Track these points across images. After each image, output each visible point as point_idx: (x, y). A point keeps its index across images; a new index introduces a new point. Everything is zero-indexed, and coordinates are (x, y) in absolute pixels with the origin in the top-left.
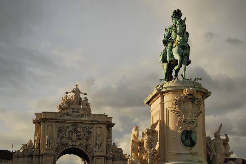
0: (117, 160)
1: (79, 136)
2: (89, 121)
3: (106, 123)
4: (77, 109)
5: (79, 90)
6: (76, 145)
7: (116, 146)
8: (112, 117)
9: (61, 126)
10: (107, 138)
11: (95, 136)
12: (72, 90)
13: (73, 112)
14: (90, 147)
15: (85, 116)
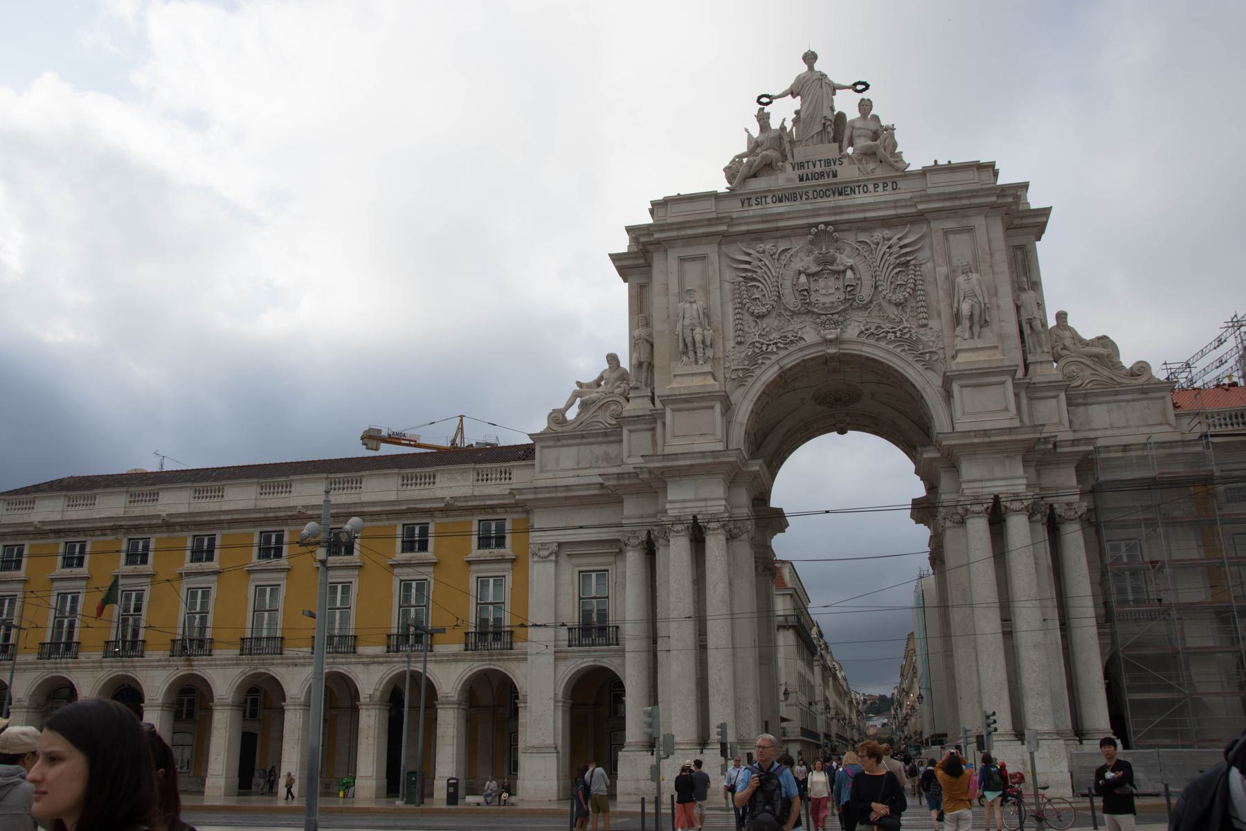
0: (1090, 400)
1: (851, 289)
2: (895, 204)
3: (994, 199)
4: (828, 162)
5: (823, 76)
6: (837, 341)
7: (1070, 329)
8: (1025, 186)
9: (749, 255)
10: (1018, 289)
11: (941, 279)
12: (787, 86)
13: (808, 179)
14: (924, 339)
15: (871, 187)
